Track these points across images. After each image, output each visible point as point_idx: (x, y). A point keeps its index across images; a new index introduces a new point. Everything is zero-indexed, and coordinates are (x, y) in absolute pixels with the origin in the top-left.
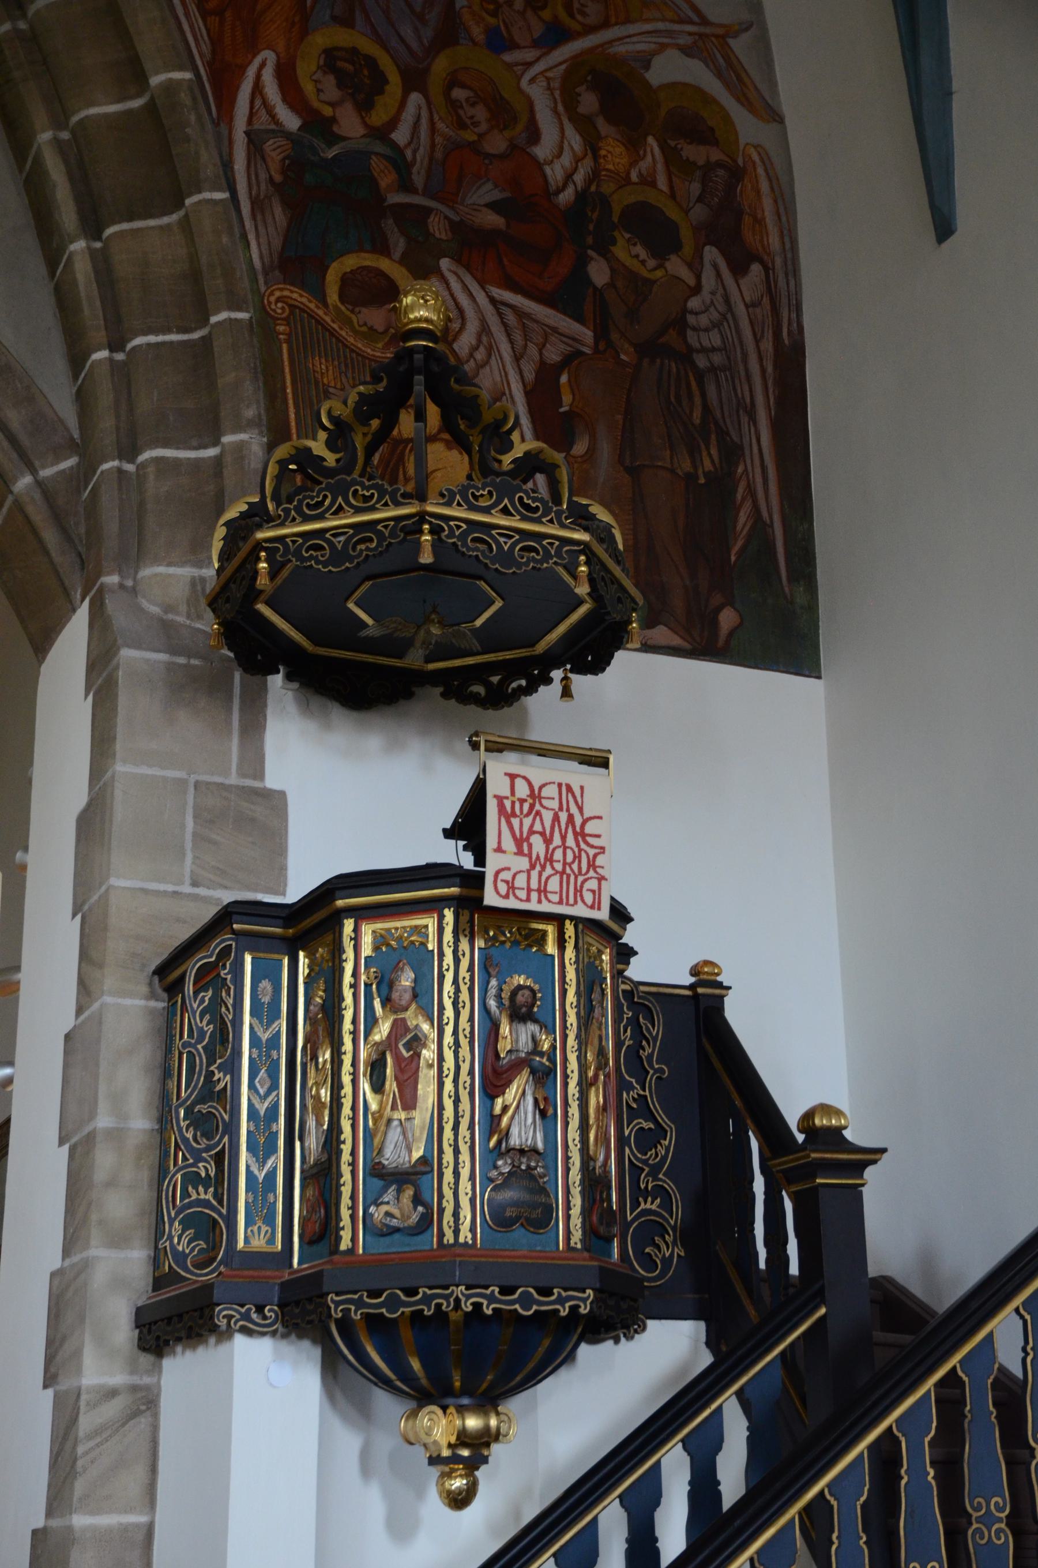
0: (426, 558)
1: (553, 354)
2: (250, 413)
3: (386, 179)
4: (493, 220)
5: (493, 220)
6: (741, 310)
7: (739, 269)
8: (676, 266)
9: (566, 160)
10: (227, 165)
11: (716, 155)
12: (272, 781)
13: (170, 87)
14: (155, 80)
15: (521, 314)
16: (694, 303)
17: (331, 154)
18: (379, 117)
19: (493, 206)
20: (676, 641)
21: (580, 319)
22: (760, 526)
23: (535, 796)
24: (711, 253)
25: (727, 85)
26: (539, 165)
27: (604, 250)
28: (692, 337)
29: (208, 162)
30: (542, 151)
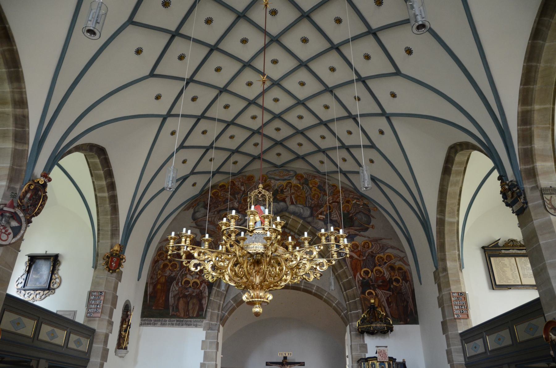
0: (372, 329)
1: (388, 296)
2: (360, 308)
3: (370, 282)
4: (381, 284)
5: (381, 284)
6: (407, 287)
7: (407, 282)
8: (400, 284)
9: (388, 275)
10: (356, 285)
11: (403, 271)
12: (365, 343)
13: (350, 278)
14: (349, 278)
15: (385, 293)
16: (402, 287)
17: (365, 281)
18: (369, 276)
19: (381, 282)
20: (403, 323)
21: (391, 292)
22: (411, 309)
23: (381, 351)
24: (403, 282)
25: (404, 263)
26: (385, 277)
27: (392, 283)
28: (402, 291)
29: (354, 285)
30: (385, 275)
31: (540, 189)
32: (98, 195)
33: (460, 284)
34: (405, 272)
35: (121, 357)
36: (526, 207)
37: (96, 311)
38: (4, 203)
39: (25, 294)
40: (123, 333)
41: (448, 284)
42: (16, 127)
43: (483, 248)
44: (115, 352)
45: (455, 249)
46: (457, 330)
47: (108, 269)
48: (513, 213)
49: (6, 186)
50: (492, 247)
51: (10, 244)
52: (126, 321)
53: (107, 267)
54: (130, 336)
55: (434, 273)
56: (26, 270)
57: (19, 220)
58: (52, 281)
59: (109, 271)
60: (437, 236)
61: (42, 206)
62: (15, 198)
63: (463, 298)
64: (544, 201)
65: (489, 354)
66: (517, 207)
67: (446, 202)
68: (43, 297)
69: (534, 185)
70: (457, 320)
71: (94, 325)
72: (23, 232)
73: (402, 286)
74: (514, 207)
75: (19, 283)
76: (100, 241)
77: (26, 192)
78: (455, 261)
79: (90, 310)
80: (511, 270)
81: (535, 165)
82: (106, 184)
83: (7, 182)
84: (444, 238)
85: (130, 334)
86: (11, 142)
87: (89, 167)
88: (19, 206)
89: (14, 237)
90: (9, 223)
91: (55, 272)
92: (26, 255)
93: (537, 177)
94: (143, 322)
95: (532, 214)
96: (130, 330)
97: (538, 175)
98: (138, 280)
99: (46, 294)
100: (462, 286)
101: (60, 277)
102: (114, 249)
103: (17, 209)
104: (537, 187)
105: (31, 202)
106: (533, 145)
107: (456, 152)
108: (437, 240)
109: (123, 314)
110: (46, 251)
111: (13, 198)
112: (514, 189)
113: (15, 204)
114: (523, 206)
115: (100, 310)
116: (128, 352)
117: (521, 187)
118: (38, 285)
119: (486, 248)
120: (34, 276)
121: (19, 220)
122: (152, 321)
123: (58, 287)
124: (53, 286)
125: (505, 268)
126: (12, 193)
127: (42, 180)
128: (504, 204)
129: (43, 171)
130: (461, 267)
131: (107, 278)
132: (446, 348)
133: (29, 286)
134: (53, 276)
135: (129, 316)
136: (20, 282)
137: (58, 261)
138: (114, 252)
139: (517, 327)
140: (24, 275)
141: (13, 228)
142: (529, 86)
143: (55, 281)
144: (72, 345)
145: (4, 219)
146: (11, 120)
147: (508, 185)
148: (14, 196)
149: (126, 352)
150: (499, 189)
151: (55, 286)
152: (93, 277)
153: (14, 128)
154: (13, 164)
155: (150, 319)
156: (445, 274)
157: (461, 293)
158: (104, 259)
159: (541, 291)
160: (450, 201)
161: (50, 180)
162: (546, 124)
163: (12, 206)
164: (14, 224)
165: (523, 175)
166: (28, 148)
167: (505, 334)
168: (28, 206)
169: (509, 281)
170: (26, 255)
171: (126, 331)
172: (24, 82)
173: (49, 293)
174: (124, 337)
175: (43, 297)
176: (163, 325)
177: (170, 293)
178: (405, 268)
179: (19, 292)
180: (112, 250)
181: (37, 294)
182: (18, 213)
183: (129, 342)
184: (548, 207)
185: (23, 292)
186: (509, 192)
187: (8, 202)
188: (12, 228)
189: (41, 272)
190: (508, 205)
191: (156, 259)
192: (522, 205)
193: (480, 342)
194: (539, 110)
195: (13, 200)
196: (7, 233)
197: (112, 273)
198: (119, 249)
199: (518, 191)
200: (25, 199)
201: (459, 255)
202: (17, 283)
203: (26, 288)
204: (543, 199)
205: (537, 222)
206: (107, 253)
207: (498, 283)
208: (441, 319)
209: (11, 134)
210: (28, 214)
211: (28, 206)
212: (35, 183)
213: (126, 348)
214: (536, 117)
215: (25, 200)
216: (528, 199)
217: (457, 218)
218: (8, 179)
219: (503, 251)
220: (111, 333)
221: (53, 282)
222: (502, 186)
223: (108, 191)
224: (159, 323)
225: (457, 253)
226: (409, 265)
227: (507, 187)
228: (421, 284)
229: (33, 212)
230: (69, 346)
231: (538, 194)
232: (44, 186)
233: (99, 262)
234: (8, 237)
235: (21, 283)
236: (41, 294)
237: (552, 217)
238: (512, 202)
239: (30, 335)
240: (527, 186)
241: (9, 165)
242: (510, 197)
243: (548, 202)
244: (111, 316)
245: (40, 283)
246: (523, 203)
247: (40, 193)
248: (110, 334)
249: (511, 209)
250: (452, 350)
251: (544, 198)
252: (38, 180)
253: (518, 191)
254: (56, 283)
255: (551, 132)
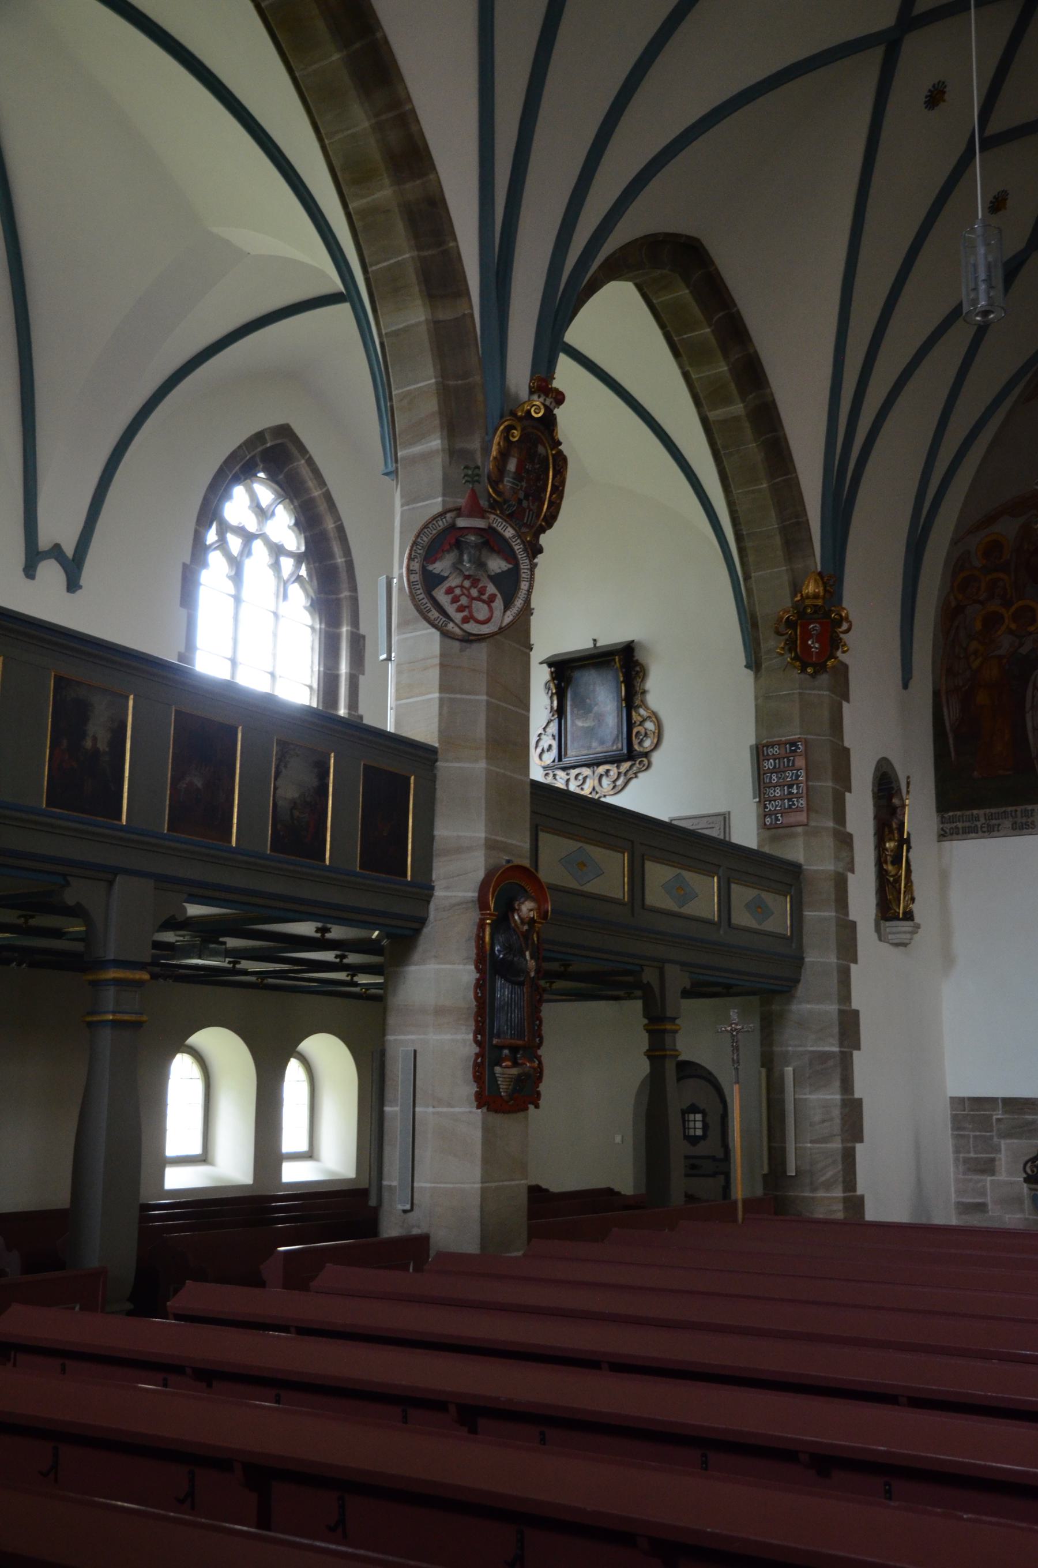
32: (713, 415)
35: (897, 945)
37: (790, 807)
38: (451, 506)
39: (568, 781)
40: (890, 868)
42: (419, 248)
44: (878, 929)
47: (798, 664)
49: (443, 450)
51: (501, 630)
52: (890, 826)
53: (796, 658)
54: (914, 877)
56: (552, 707)
57: (505, 551)
58: (635, 731)
59: (803, 670)
61: (559, 490)
62: (478, 482)
68: (620, 782)
71: (796, 852)
72: (527, 584)
75: (543, 750)
76: (753, 574)
77: (504, 456)
79: (770, 807)
82: (730, 370)
83: (442, 439)
85: (913, 867)
86: (419, 302)
87: (662, 326)
88: (494, 506)
89: (507, 606)
90: (481, 565)
91: (637, 702)
92: (541, 663)
94: (948, 826)
96: (911, 855)
98: (905, 686)
99: (626, 774)
101: (655, 714)
102: (805, 592)
103: (492, 517)
105: (524, 484)
109: (877, 806)
110: (595, 640)
111: (473, 482)
113: (484, 503)
115: (803, 802)
116: (918, 927)
118: (597, 749)
120: (580, 723)
121: (505, 551)
122: (978, 819)
123: (657, 746)
124: (640, 743)
126: (466, 467)
127: (537, 403)
129: (533, 373)
131: (800, 694)
133: (574, 753)
134: (634, 713)
135: (899, 811)
136: (545, 749)
137: (637, 663)
138: (808, 602)
140: (552, 725)
141: (496, 579)
143: (640, 728)
144: (742, 918)
145: (466, 557)
146: (400, 227)
148: (473, 477)
149: (910, 929)
151: (648, 744)
152: (756, 698)
153: (415, 253)
154: (443, 374)
155: (968, 813)
158: (778, 633)
161: (559, 398)
163: (475, 510)
164: (497, 565)
166: (471, 307)
168: (520, 501)
170: (541, 663)
171: (897, 860)
172: (402, 80)
173: (635, 769)
174: (898, 880)
175: (620, 782)
176: (1022, 828)
177: (1028, 717)
179: (551, 775)
180: (798, 598)
181: (601, 776)
182: (499, 529)
183: (916, 894)
185: (561, 774)
187: (461, 501)
188: (495, 579)
189: (596, 709)
191: (953, 604)
195: (473, 491)
196: (485, 597)
197: (813, 676)
198: (820, 590)
200: (506, 479)
202: (539, 750)
203: (567, 761)
206: (786, 611)
209: (412, 277)
210: (525, 525)
211: (520, 501)
212: (520, 419)
213: (909, 916)
215: (507, 482)
218: (442, 428)
220: (853, 871)
221: (638, 733)
223: (743, 395)
224: (1007, 823)
229: (538, 516)
230: (734, 921)
232: (549, 421)
233: (764, 647)
234: (491, 609)
235: (550, 746)
236: (611, 773)
239: (621, 896)
241: (433, 381)
244: (840, 816)
245: (602, 742)
247: (541, 449)
248: (850, 875)
252: (527, 407)
254: (646, 735)
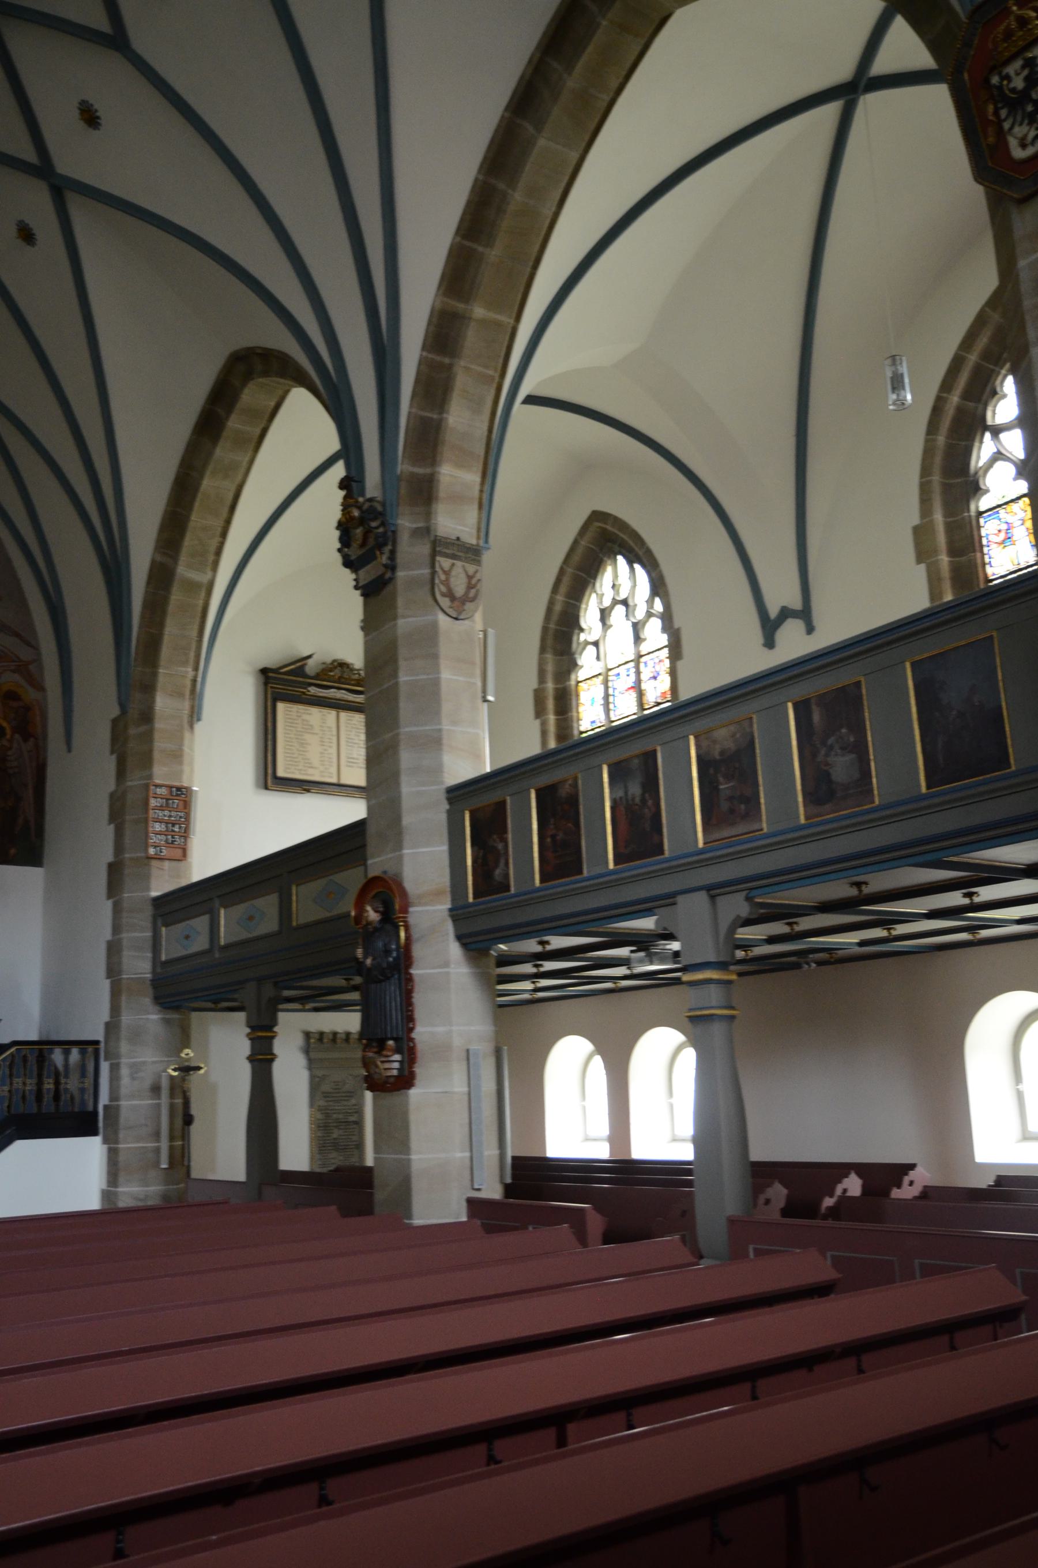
7: (25, 740)
16: (9, 753)
24: (17, 736)
31: (432, 538)
33: (181, 763)
34: (28, 708)
36: (391, 579)
41: (147, 760)
43: (264, 672)
45: (185, 663)
46: (148, 889)
48: (356, 588)
50: (285, 673)
55: (115, 722)
60: (143, 616)
63: (181, 804)
64: (434, 573)
65: (217, 955)
66: (367, 574)
67: (187, 518)
69: (421, 525)
70: (154, 863)
73: (10, 748)
74: (361, 572)
78: (181, 695)
80: (322, 742)
81: (438, 469)
84: (161, 625)
93: (434, 506)
95: (400, 602)
97: (437, 498)
100: (186, 768)
104: (425, 532)
106: (445, 415)
107: (248, 376)
108: (140, 627)
112: (374, 524)
114: (383, 575)
117: (391, 521)
119: (271, 674)
125: (307, 737)
128: (338, 558)
130: (195, 714)
132: (108, 935)
139: (302, 888)
142: (475, 246)
147: (359, 508)
150: (335, 512)
156: (143, 728)
157: (179, 789)
159: (373, 802)
160: (197, 519)
162: (486, 367)
165: (403, 491)
167: (268, 905)
169: (310, 771)
178: (30, 694)
184: (440, 590)
186: (356, 528)
190: (348, 563)
192: (381, 570)
193: (201, 923)
194: (483, 322)
199: (381, 530)
201: (194, 681)
204: (433, 565)
205: (405, 623)
207: (281, 773)
208: (110, 857)
214: (472, 339)
216: (401, 558)
217: (209, 574)
219: (313, 690)
222: (346, 506)
225: (191, 674)
226: (41, 688)
227: (356, 513)
228: (69, 750)
231: (425, 549)
237: (442, 618)
238: (359, 558)
240: (405, 522)
242: (359, 542)
243: (443, 577)
246: (386, 566)
249: (354, 576)
250: (125, 943)
251: (437, 565)
253: (381, 530)
255: (493, 392)
